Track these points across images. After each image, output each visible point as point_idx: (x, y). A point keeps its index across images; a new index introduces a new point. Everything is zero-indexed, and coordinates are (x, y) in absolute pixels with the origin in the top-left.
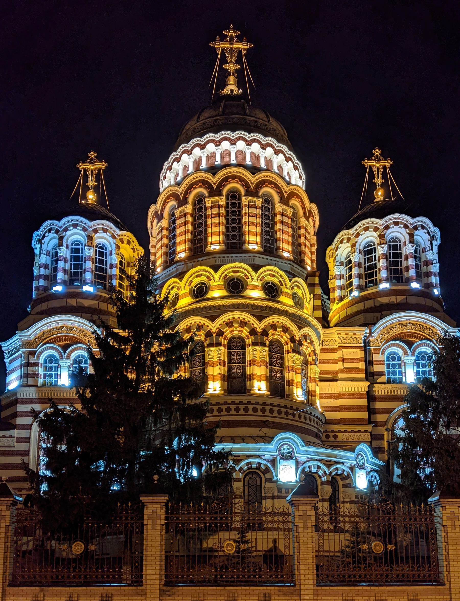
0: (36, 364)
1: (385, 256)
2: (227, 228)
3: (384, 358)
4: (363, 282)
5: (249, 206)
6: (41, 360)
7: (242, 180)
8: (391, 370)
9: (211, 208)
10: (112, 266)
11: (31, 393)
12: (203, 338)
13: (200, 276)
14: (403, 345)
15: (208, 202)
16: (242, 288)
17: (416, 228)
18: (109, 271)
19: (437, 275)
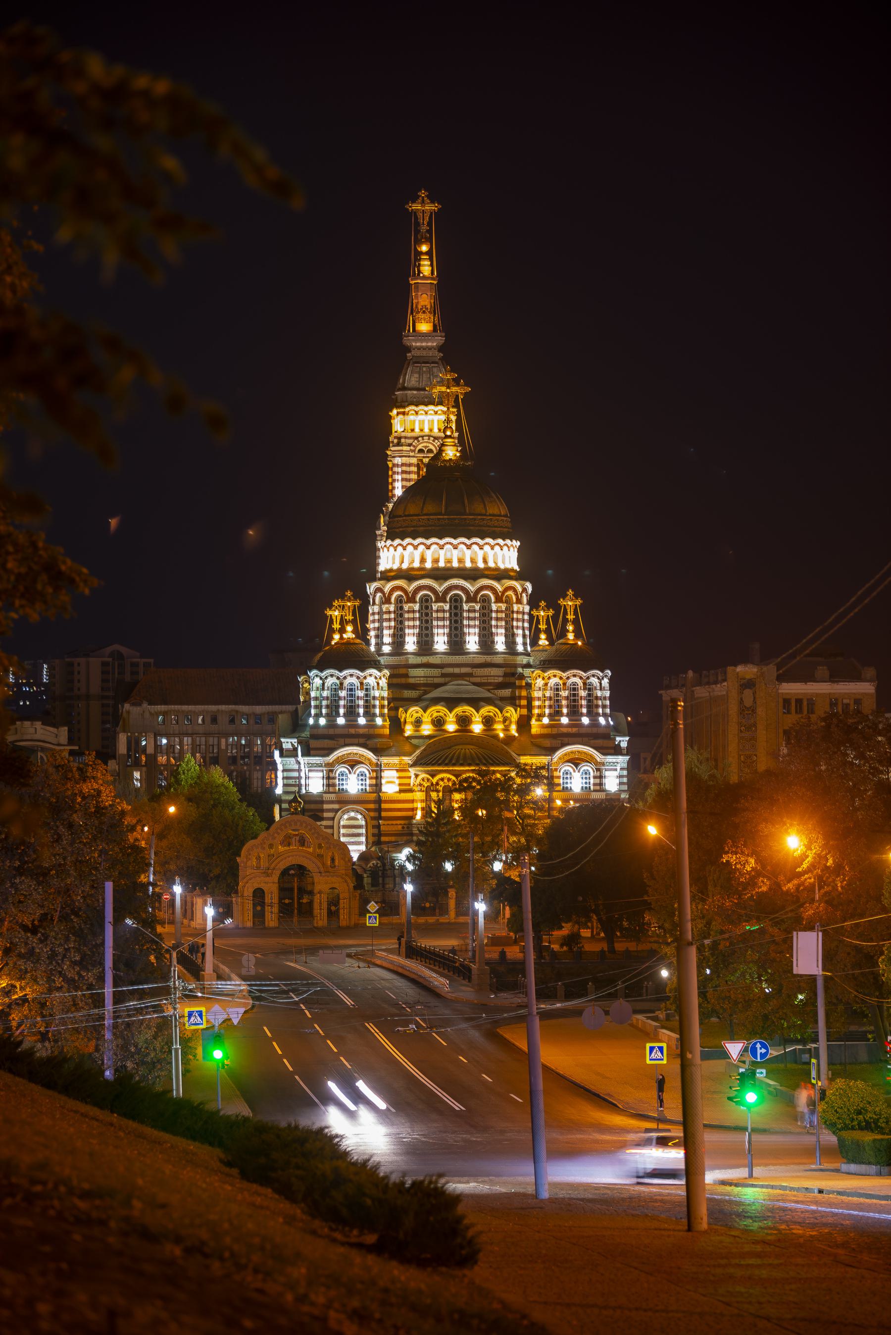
0: (334, 778)
1: (567, 698)
2: (450, 628)
3: (561, 774)
4: (552, 711)
5: (469, 611)
6: (337, 775)
7: (463, 589)
8: (565, 781)
9: (437, 611)
10: (374, 698)
11: (332, 797)
12: (450, 785)
13: (439, 712)
14: (573, 766)
15: (435, 607)
16: (469, 722)
17: (588, 678)
18: (372, 702)
19: (607, 698)
